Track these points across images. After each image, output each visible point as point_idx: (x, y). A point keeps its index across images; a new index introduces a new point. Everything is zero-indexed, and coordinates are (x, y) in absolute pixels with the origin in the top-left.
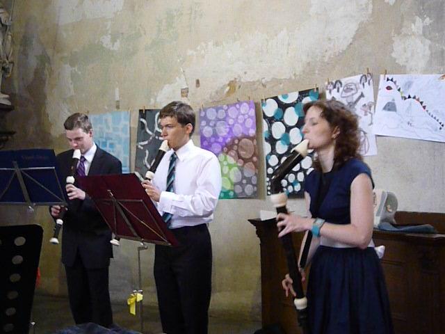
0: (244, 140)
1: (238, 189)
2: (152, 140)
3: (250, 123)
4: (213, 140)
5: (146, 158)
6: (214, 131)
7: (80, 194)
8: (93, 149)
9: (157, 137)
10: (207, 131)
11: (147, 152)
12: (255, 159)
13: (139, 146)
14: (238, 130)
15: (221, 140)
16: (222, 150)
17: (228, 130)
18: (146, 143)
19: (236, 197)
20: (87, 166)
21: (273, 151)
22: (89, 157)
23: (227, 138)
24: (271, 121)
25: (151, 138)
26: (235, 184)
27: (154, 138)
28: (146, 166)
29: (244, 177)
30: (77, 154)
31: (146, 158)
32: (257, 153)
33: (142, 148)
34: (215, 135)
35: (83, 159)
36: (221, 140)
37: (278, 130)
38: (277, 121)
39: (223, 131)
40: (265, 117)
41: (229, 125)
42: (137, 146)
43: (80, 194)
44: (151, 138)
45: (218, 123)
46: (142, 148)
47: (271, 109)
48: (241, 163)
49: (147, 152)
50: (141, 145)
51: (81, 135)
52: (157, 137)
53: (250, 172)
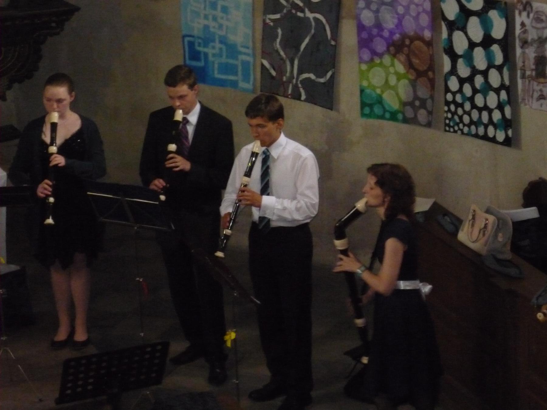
0: (417, 43)
1: (409, 113)
2: (286, 14)
3: (425, 20)
4: (375, 31)
5: (278, 40)
6: (377, 18)
7: (182, 164)
9: (294, 11)
10: (367, 18)
11: (280, 31)
12: (430, 74)
13: (268, 21)
14: (410, 26)
15: (386, 34)
16: (388, 48)
17: (396, 21)
18: (278, 16)
20: (191, 129)
21: (453, 71)
23: (395, 34)
24: (452, 26)
25: (285, 11)
26: (404, 104)
27: (289, 12)
28: (277, 51)
29: (416, 97)
31: (278, 40)
33: (272, 24)
34: (379, 26)
35: (186, 121)
36: (386, 34)
37: (460, 43)
38: (458, 29)
39: (389, 21)
40: (445, 19)
42: (264, 21)
43: (182, 164)
44: (285, 11)
45: (383, 7)
46: (272, 24)
47: (451, 10)
49: (280, 31)
50: (270, 19)
52: (294, 11)
53: (423, 92)
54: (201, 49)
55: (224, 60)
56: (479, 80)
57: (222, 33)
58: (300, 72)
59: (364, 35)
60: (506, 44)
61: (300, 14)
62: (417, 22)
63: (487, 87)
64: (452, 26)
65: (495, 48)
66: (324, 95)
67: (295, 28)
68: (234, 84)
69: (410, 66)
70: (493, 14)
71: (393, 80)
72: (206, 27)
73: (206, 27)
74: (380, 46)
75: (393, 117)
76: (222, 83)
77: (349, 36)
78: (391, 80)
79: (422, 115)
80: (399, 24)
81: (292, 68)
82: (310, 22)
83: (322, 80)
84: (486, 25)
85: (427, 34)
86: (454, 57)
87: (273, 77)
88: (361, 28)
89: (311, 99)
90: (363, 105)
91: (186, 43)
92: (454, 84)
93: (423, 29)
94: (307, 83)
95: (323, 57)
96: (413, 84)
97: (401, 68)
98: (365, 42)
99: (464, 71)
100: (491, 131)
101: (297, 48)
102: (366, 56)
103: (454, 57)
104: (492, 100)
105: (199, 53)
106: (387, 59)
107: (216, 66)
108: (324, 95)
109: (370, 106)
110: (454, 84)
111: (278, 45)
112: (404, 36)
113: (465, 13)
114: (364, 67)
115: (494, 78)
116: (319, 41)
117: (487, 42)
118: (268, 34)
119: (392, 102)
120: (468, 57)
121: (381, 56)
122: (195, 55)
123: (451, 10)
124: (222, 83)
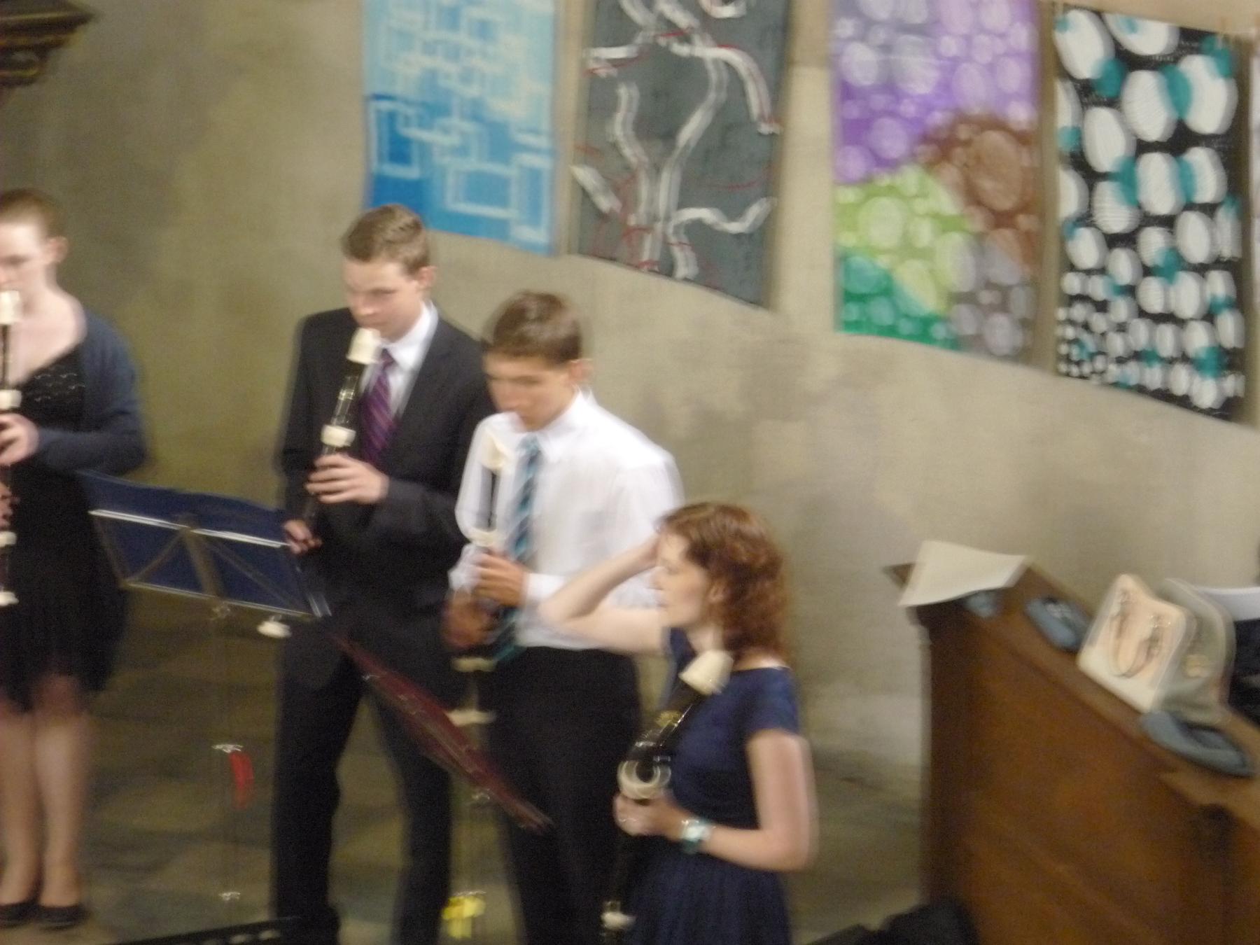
0: (994, 138)
1: (966, 321)
3: (1016, 75)
4: (880, 101)
8: (425, 325)
12: (1024, 221)
14: (975, 92)
17: (933, 75)
18: (619, 53)
19: (956, 343)
20: (398, 384)
21: (1086, 219)
22: (409, 353)
24: (1088, 93)
28: (615, 146)
30: (365, 348)
31: (619, 117)
32: (1036, 201)
34: (890, 86)
35: (387, 361)
36: (908, 109)
37: (1107, 147)
39: (920, 75)
40: (1066, 75)
41: (938, 56)
42: (583, 62)
47: (1084, 50)
48: (977, 222)
50: (597, 59)
51: (389, 284)
53: (1007, 267)
54: (414, 133)
55: (473, 163)
56: (1153, 242)
57: (473, 91)
58: (682, 205)
59: (854, 111)
60: (1232, 147)
61: (681, 50)
62: (995, 78)
63: (1176, 264)
64: (1088, 93)
65: (1201, 160)
66: (742, 268)
67: (668, 86)
68: (499, 230)
69: (972, 196)
70: (1198, 68)
71: (925, 234)
72: (431, 76)
73: (431, 76)
74: (893, 140)
75: (923, 330)
76: (467, 226)
77: (811, 110)
78: (919, 233)
79: (1002, 332)
80: (946, 86)
81: (657, 194)
82: (706, 72)
83: (735, 227)
84: (1178, 93)
85: (1020, 114)
86: (1090, 176)
87: (602, 217)
88: (845, 91)
89: (707, 278)
90: (848, 297)
91: (373, 116)
92: (1086, 248)
93: (1006, 98)
94: (696, 231)
95: (742, 163)
96: (979, 243)
97: (945, 201)
98: (855, 126)
99: (1115, 217)
100: (1182, 380)
101: (669, 135)
102: (856, 163)
103: (1090, 176)
104: (1187, 295)
105: (406, 142)
106: (910, 178)
107: (450, 180)
108: (742, 268)
109: (863, 299)
110: (1086, 248)
111: (620, 127)
112: (962, 118)
113: (1127, 61)
114: (849, 195)
115: (1197, 238)
116: (731, 121)
117: (1180, 140)
118: (597, 98)
119: (922, 294)
120: (1127, 178)
121: (890, 165)
122: (399, 150)
123: (1084, 50)
124: (467, 226)
